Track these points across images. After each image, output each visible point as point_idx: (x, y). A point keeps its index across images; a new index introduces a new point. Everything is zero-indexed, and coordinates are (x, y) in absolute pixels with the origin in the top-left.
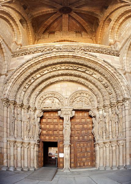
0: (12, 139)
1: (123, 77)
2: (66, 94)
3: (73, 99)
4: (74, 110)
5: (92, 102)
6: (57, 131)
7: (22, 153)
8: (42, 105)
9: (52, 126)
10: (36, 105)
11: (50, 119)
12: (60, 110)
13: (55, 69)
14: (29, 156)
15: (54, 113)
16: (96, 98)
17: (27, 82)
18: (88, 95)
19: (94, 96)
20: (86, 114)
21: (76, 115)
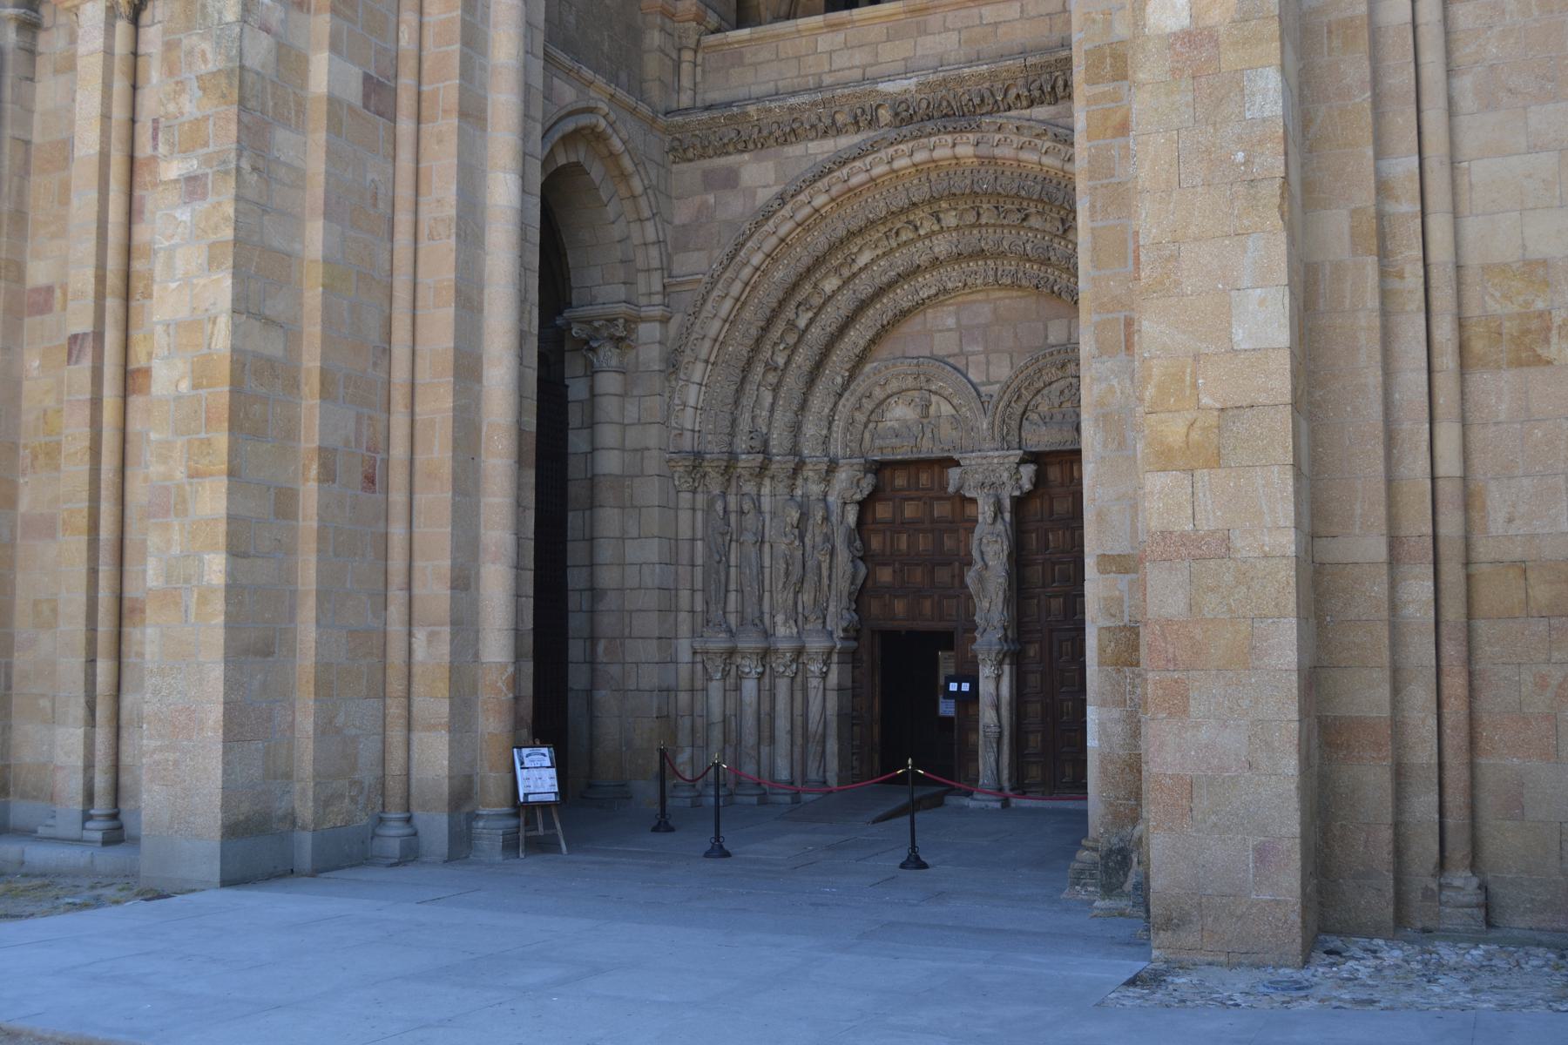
0: (718, 642)
2: (988, 375)
3: (1026, 395)
4: (1032, 457)
6: (950, 564)
7: (765, 707)
8: (867, 436)
9: (923, 543)
10: (836, 448)
11: (912, 499)
12: (957, 464)
13: (911, 235)
14: (799, 721)
17: (775, 334)
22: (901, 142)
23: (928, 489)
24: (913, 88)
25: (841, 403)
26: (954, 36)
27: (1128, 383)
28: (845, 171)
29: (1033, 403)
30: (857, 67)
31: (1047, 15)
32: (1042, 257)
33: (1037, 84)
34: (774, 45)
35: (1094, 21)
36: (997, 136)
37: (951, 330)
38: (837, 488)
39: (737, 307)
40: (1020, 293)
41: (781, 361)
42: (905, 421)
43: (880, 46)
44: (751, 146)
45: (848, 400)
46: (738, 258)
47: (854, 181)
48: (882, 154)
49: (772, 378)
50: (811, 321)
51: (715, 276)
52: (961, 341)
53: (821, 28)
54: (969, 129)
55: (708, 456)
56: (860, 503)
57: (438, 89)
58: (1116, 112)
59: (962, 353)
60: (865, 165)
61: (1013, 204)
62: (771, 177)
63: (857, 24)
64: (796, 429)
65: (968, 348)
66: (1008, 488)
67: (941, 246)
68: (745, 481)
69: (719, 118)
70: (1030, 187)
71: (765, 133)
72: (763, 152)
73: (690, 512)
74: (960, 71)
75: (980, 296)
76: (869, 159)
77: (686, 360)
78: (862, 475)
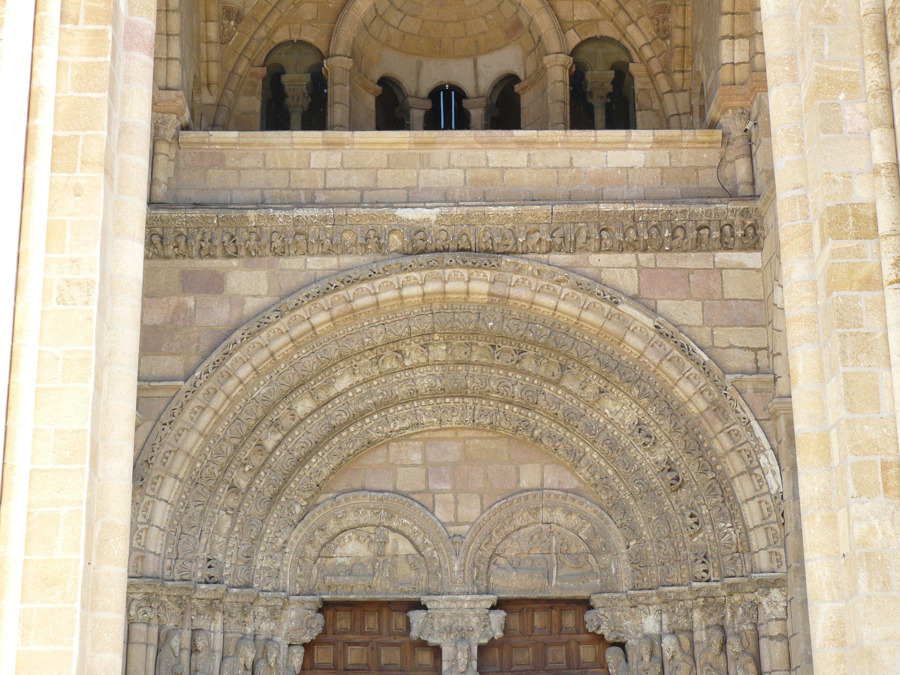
1: (757, 439)
2: (456, 515)
3: (496, 538)
4: (500, 605)
5: (605, 559)
11: (357, 644)
12: (418, 605)
13: (395, 365)
15: (385, 612)
16: (621, 539)
18: (574, 517)
19: (613, 526)
20: (569, 620)
21: (515, 620)
22: (413, 271)
23: (374, 634)
24: (434, 218)
25: (293, 535)
26: (459, 174)
27: (888, 524)
28: (351, 291)
29: (501, 547)
30: (355, 189)
31: (555, 168)
32: (531, 400)
33: (560, 232)
34: (260, 153)
35: (835, 181)
36: (515, 277)
37: (415, 466)
38: (286, 627)
39: (214, 421)
40: (491, 434)
41: (243, 484)
42: (358, 558)
43: (379, 172)
44: (242, 252)
45: (300, 531)
46: (223, 368)
47: (359, 303)
48: (393, 279)
49: (232, 501)
50: (279, 443)
51: (198, 384)
52: (427, 477)
53: (317, 144)
54: (488, 265)
55: (170, 583)
56: (305, 645)
57: (77, 137)
58: (861, 268)
59: (427, 491)
60: (374, 288)
61: (511, 345)
62: (263, 289)
63: (356, 147)
64: (249, 558)
65: (434, 486)
66: (477, 634)
67: (424, 381)
68: (199, 614)
69: (212, 218)
70: (538, 329)
71: (264, 240)
72: (256, 260)
73: (144, 646)
74: (486, 209)
75: (448, 434)
76: (377, 283)
77: (155, 474)
78: (313, 615)
